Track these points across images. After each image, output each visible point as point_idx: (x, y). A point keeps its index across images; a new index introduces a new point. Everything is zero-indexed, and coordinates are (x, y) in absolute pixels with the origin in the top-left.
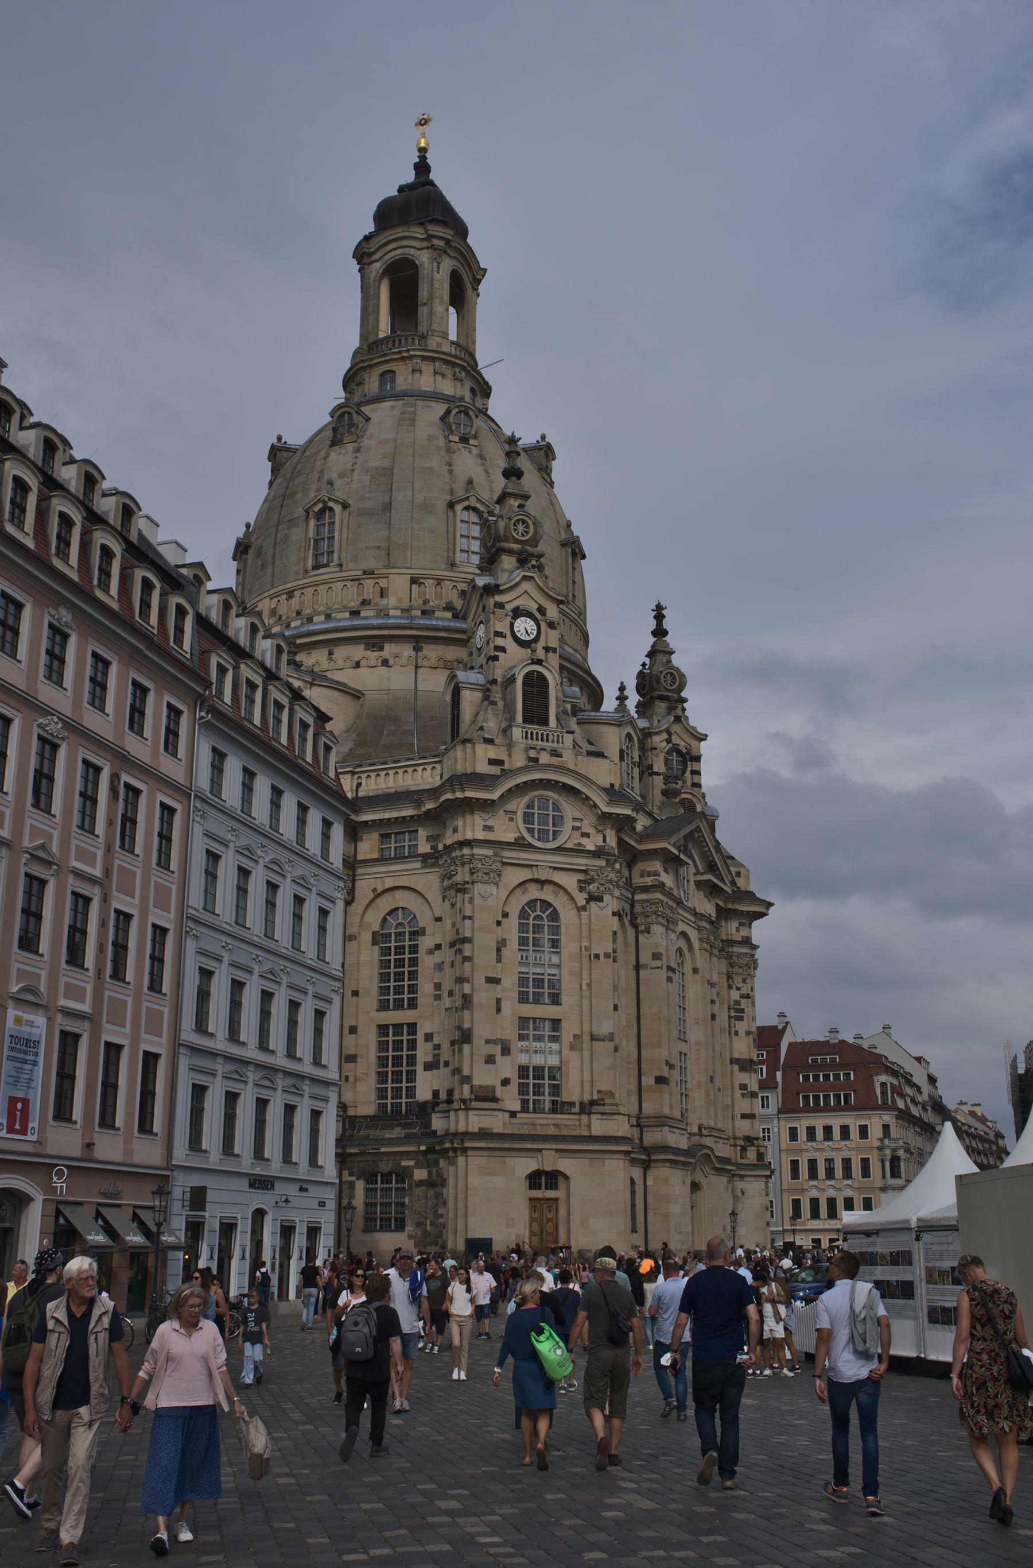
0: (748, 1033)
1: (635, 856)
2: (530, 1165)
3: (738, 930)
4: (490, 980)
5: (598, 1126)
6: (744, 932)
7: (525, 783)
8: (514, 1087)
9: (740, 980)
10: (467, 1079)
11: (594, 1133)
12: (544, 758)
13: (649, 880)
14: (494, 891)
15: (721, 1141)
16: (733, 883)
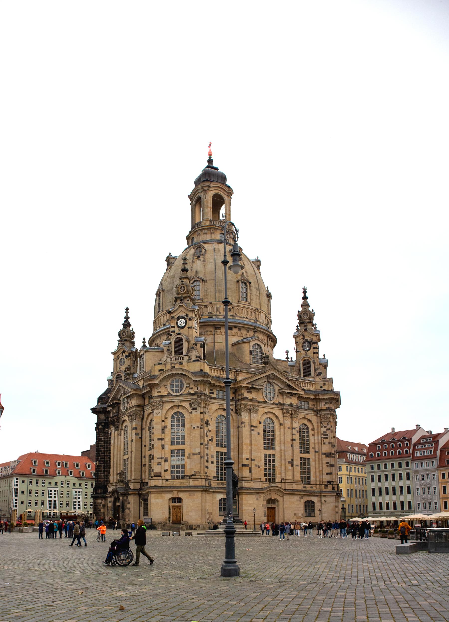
0: (329, 443)
1: (236, 390)
2: (169, 496)
3: (324, 405)
4: (159, 439)
5: (192, 482)
6: (327, 406)
7: (168, 375)
8: (169, 472)
9: (326, 423)
10: (153, 470)
11: (191, 485)
12: (177, 366)
13: (240, 397)
14: (160, 411)
15: (295, 484)
16: (303, 390)
